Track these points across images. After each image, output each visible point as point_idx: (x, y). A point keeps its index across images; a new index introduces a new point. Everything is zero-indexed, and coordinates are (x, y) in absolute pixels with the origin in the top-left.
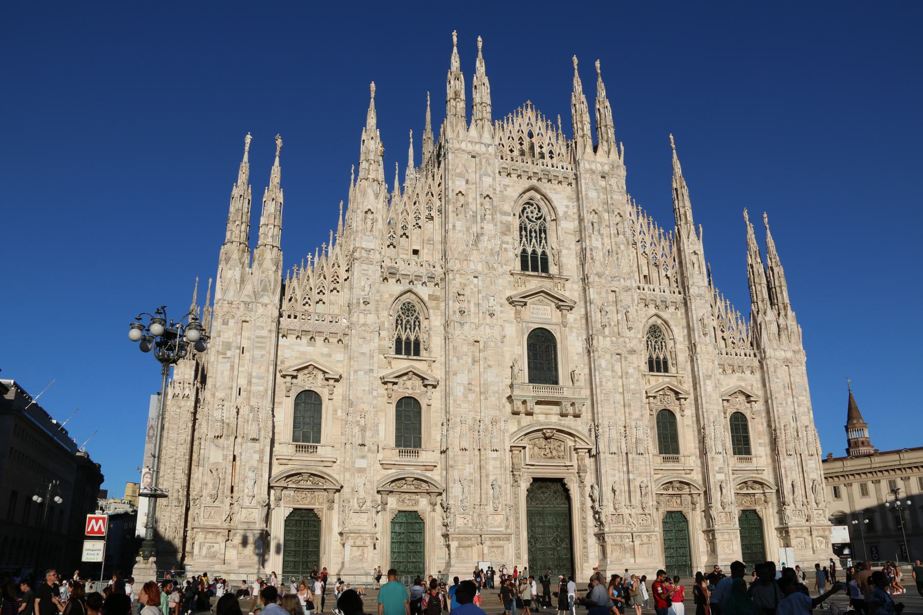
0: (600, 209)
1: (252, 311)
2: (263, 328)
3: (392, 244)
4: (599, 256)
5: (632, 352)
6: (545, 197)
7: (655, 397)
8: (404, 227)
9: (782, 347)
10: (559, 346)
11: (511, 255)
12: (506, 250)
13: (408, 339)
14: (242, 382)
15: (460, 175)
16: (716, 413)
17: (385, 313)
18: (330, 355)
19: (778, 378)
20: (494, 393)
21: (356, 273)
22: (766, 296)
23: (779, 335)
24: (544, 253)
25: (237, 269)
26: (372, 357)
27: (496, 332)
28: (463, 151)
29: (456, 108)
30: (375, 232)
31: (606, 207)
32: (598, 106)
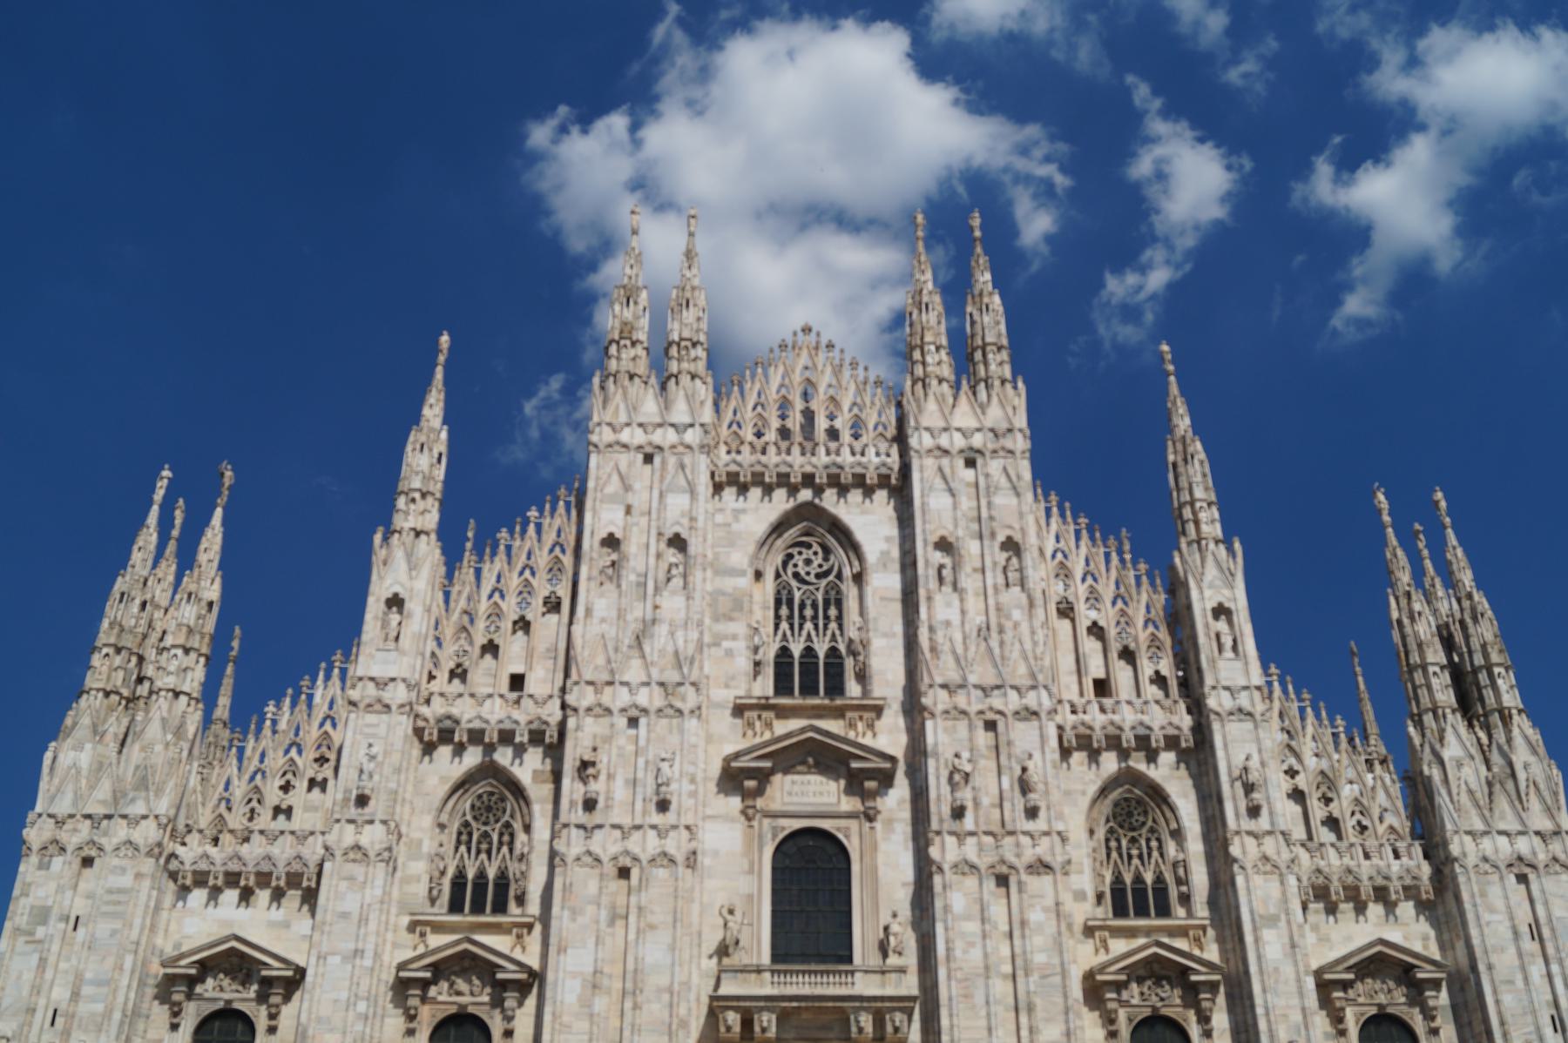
2: (123, 870)
5: (1041, 867)
7: (1119, 986)
10: (855, 868)
11: (743, 663)
12: (729, 653)
14: (60, 994)
15: (612, 499)
16: (1297, 1017)
17: (427, 821)
18: (286, 925)
19: (1492, 911)
20: (659, 991)
22: (1446, 696)
23: (1491, 794)
24: (833, 652)
25: (88, 746)
26: (363, 920)
28: (625, 446)
30: (405, 642)
31: (975, 526)
32: (969, 309)
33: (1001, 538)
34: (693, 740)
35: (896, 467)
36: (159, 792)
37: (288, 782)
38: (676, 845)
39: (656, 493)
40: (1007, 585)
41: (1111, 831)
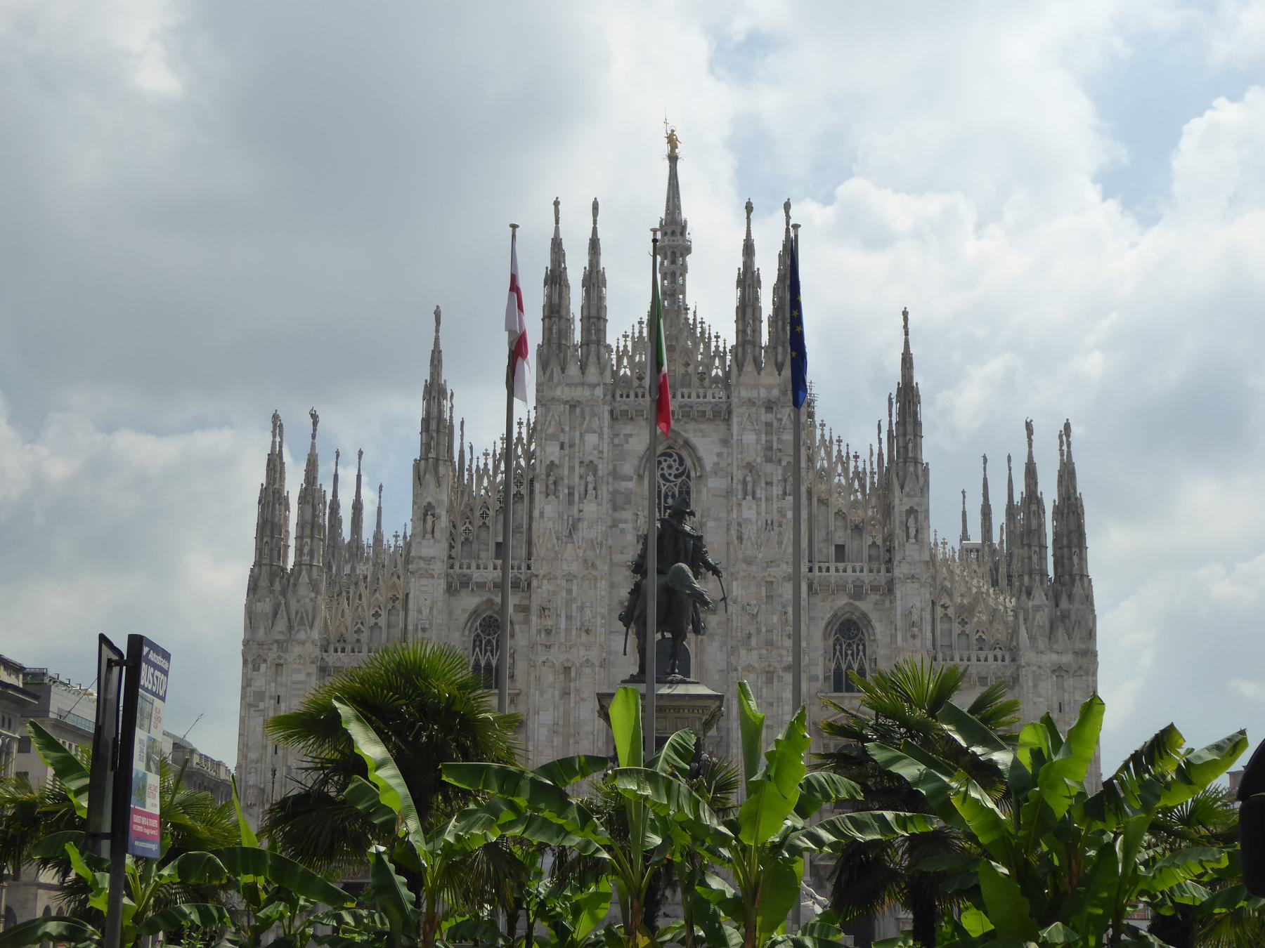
0: (759, 460)
1: (286, 651)
3: (467, 539)
4: (750, 531)
6: (687, 444)
8: (484, 515)
9: (1055, 647)
12: (623, 531)
13: (488, 664)
15: (552, 437)
17: (457, 635)
19: (1039, 696)
21: (412, 592)
23: (1052, 628)
27: (594, 655)
29: (550, 330)
30: (437, 534)
31: (769, 453)
33: (784, 463)
34: (603, 593)
35: (724, 407)
36: (311, 627)
37: (376, 615)
38: (594, 655)
39: (577, 434)
40: (785, 493)
41: (837, 639)
